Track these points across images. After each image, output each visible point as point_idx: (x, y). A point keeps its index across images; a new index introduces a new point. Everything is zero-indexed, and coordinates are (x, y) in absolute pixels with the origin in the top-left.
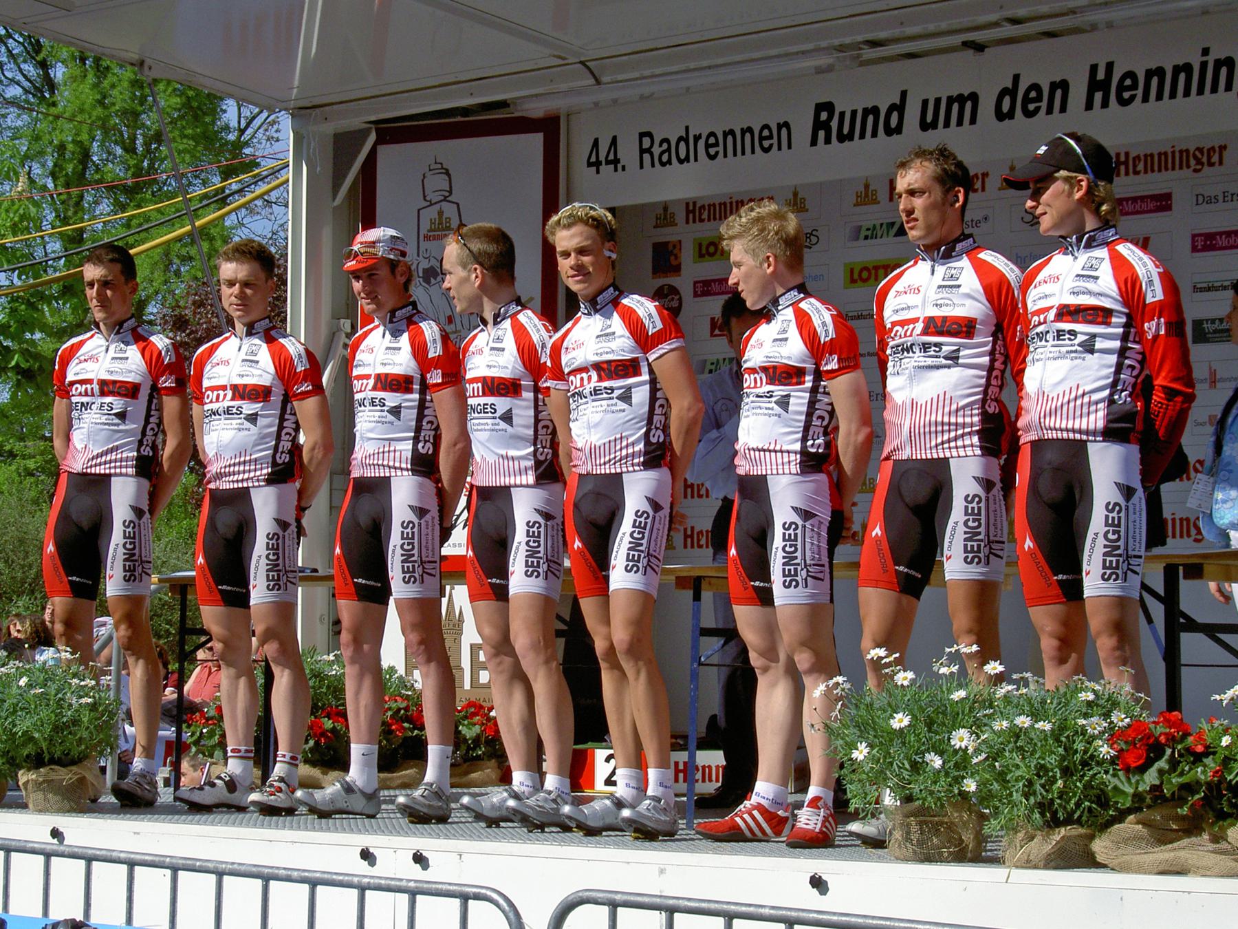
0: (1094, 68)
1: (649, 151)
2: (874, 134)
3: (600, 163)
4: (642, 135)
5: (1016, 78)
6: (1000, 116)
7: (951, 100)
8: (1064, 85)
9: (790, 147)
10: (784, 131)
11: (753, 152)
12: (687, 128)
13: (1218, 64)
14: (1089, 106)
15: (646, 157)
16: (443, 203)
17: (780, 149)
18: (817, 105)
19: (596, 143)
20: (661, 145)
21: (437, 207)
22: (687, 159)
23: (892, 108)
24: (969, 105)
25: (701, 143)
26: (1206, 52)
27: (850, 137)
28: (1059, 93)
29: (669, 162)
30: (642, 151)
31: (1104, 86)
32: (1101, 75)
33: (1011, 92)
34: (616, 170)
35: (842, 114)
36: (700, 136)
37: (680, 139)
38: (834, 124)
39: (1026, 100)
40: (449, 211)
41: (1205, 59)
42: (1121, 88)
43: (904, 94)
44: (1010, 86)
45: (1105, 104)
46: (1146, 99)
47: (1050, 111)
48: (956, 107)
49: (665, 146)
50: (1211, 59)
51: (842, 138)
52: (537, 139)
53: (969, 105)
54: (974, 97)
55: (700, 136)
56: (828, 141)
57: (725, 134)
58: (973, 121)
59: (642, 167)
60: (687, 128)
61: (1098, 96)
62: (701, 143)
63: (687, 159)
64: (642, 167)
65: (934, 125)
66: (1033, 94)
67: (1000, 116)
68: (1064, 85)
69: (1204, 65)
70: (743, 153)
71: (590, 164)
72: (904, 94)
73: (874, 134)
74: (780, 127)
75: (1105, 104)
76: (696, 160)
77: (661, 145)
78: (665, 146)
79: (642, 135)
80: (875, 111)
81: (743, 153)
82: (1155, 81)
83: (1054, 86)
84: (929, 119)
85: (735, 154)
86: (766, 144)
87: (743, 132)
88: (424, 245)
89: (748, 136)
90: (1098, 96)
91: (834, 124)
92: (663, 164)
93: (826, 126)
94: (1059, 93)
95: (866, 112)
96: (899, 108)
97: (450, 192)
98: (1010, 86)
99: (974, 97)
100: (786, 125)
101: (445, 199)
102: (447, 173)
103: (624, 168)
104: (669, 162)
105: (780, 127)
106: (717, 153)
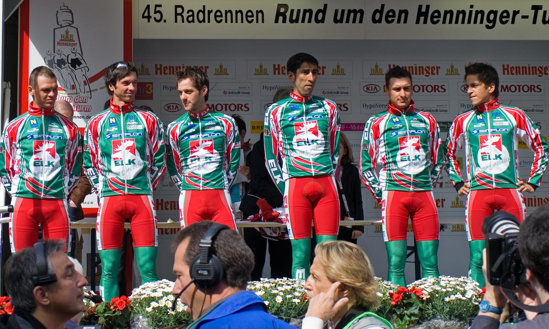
0: (420, 7)
1: (181, 14)
2: (310, 21)
3: (151, 17)
4: (176, 7)
5: (383, 6)
6: (374, 21)
7: (350, 12)
8: (406, 12)
9: (263, 22)
10: (260, 14)
11: (242, 22)
12: (204, 6)
13: (477, 12)
14: (418, 22)
15: (179, 17)
17: (257, 22)
18: (279, 5)
19: (148, 7)
20: (188, 12)
21: (65, 28)
22: (204, 21)
23: (319, 11)
24: (359, 15)
25: (212, 15)
26: (472, 7)
27: (297, 21)
29: (193, 21)
30: (177, 14)
31: (425, 14)
32: (423, 10)
33: (381, 12)
35: (292, 11)
36: (212, 11)
38: (288, 14)
39: (387, 16)
40: (72, 31)
41: (471, 9)
42: (433, 17)
43: (326, 6)
44: (380, 9)
45: (425, 22)
47: (399, 22)
48: (352, 15)
49: (191, 13)
50: (474, 10)
51: (291, 21)
53: (359, 15)
54: (361, 12)
55: (212, 11)
56: (284, 21)
57: (226, 12)
58: (361, 21)
59: (176, 21)
60: (204, 6)
61: (422, 19)
62: (212, 15)
63: (204, 21)
64: (176, 21)
65: (341, 21)
67: (374, 21)
68: (406, 12)
69: (471, 12)
70: (237, 22)
71: (144, 17)
72: (326, 6)
73: (310, 21)
74: (258, 12)
75: (425, 22)
76: (209, 22)
77: (188, 12)
78: (191, 13)
79: (176, 7)
80: (310, 11)
81: (237, 22)
82: (448, 16)
83: (401, 12)
84: (339, 18)
85: (232, 22)
86: (250, 19)
87: (237, 12)
89: (239, 14)
90: (422, 19)
91: (288, 14)
93: (284, 15)
95: (305, 11)
96: (324, 11)
97: (73, 22)
98: (380, 9)
99: (361, 12)
100: (261, 12)
101: (70, 25)
102: (71, 12)
103: (165, 21)
104: (193, 21)
105: (258, 12)
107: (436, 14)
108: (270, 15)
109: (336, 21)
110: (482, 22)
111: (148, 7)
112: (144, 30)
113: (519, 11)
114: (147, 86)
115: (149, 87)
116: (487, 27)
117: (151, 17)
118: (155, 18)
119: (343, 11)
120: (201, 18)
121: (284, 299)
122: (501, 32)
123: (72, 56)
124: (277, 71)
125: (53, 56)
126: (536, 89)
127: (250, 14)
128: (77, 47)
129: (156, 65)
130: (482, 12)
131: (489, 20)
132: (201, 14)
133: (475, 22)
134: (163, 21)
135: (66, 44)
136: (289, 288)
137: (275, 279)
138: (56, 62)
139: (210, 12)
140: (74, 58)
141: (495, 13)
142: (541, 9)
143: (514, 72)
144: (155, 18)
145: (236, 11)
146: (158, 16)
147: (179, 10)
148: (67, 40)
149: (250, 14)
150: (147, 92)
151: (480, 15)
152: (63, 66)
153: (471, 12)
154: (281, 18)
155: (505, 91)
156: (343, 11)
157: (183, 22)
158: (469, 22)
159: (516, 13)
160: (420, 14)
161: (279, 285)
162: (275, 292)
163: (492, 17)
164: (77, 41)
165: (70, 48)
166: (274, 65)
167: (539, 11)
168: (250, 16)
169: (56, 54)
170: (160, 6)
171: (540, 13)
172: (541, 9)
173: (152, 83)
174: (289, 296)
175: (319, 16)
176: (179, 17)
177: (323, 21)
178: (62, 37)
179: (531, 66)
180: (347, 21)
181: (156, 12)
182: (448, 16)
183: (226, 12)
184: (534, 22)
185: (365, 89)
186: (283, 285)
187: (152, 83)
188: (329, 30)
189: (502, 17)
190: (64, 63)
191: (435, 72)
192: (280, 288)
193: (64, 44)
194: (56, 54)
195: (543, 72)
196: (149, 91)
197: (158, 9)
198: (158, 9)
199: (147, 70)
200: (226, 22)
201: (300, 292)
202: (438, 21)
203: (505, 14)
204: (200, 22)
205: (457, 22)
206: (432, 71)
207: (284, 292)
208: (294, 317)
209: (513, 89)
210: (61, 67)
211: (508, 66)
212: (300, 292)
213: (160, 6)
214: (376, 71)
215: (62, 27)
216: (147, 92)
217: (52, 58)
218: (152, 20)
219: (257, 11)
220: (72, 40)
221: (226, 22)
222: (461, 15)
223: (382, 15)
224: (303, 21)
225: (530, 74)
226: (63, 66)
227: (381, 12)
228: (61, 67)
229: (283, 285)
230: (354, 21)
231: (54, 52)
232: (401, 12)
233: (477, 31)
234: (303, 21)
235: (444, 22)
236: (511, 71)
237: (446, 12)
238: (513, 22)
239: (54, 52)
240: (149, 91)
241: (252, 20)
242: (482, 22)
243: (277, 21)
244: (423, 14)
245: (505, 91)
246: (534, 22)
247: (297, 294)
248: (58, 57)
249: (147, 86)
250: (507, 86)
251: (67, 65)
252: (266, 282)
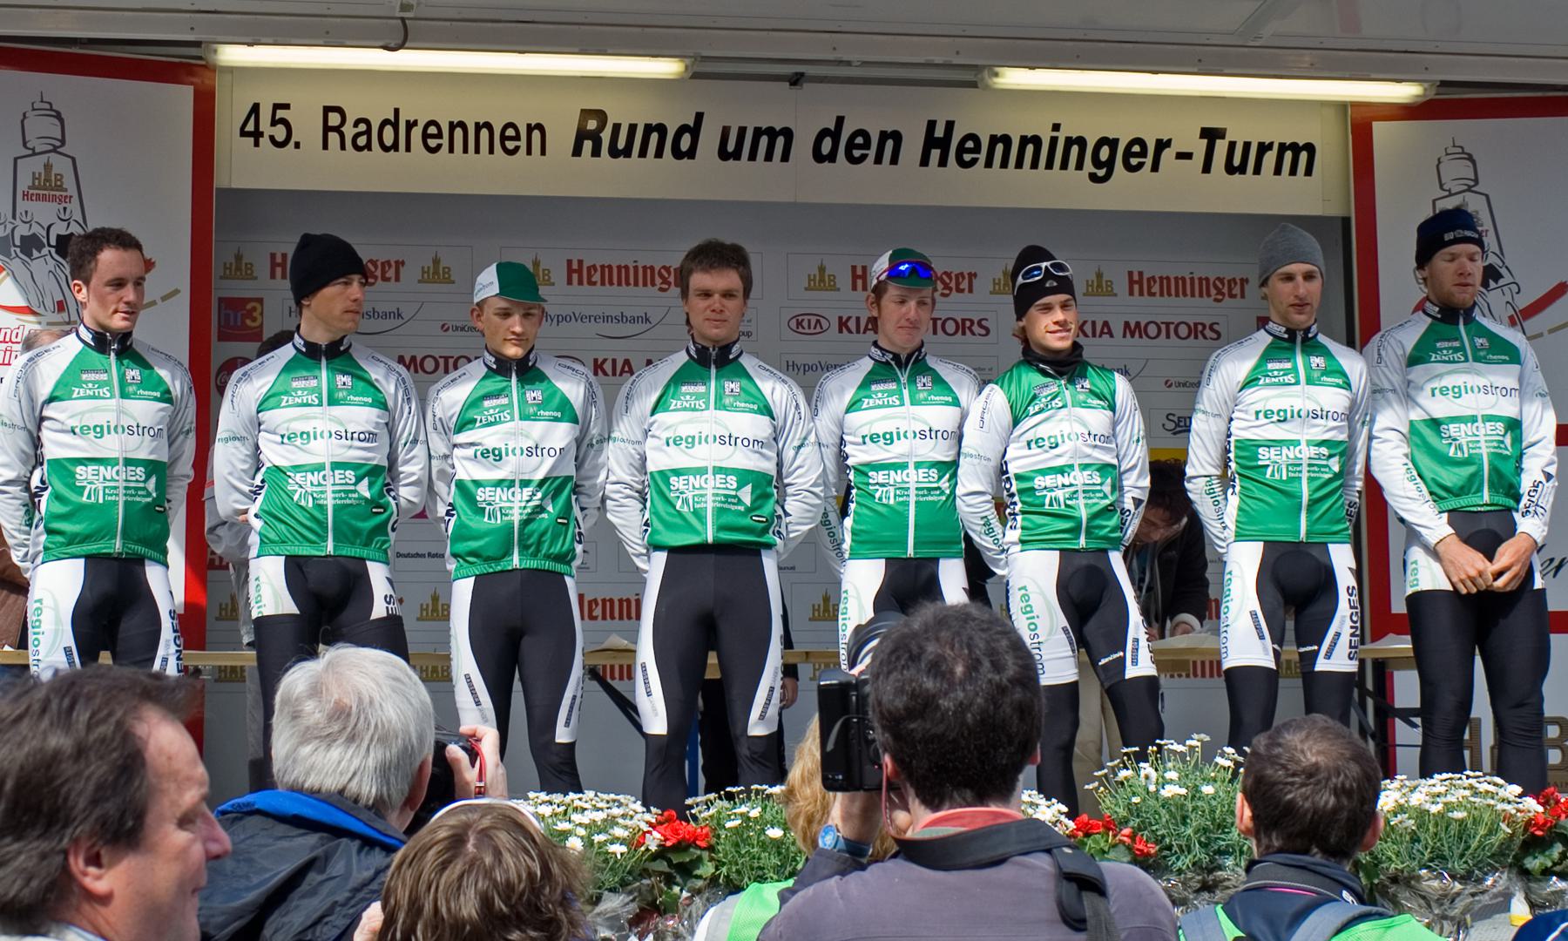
0: (932, 125)
1: (337, 129)
2: (659, 154)
3: (262, 134)
4: (327, 110)
5: (840, 121)
6: (818, 157)
7: (758, 132)
8: (897, 137)
9: (543, 152)
10: (536, 134)
11: (491, 151)
12: (397, 111)
13: (1069, 142)
14: (925, 162)
15: (334, 137)
16: (53, 157)
19: (255, 109)
20: (356, 125)
22: (395, 147)
23: (683, 129)
24: (780, 141)
25: (417, 133)
26: (1056, 127)
27: (627, 152)
28: (890, 144)
29: (368, 146)
30: (327, 129)
31: (944, 144)
32: (939, 132)
34: (257, 144)
35: (617, 127)
36: (415, 123)
37: (385, 122)
38: (606, 136)
39: (851, 145)
40: (61, 165)
42: (961, 149)
43: (699, 117)
45: (943, 162)
46: (878, 160)
47: (878, 160)
48: (764, 140)
49: (362, 127)
51: (614, 152)
52: (181, 97)
53: (780, 141)
54: (788, 133)
55: (415, 123)
56: (596, 152)
57: (452, 126)
59: (325, 147)
60: (397, 111)
61: (935, 154)
62: (417, 133)
63: (395, 147)
64: (325, 147)
65: (737, 155)
66: (859, 140)
67: (818, 157)
68: (897, 137)
69: (1054, 141)
70: (477, 151)
71: (243, 133)
72: (699, 117)
73: (659, 154)
74: (530, 129)
75: (943, 162)
76: (408, 149)
77: (356, 125)
78: (362, 127)
79: (327, 110)
80: (661, 129)
81: (477, 151)
82: (1000, 147)
83: (884, 136)
84: (731, 147)
85: (465, 150)
86: (510, 145)
87: (478, 127)
88: (22, 205)
89: (484, 133)
90: (935, 154)
91: (606, 136)
92: (358, 148)
94: (890, 144)
95: (649, 129)
96: (695, 131)
99: (788, 133)
100: (540, 127)
101: (55, 150)
102: (58, 116)
103: (297, 145)
104: (368, 146)
106: (439, 146)
107: (970, 144)
108: (562, 135)
109: (724, 154)
110: (1079, 166)
111: (255, 109)
112: (244, 166)
113: (1169, 141)
114: (249, 306)
115: (254, 309)
116: (1094, 178)
117: (262, 134)
118: (272, 138)
119: (742, 131)
120: (388, 141)
121: (589, 843)
122: (1128, 191)
123: (60, 229)
124: (575, 276)
125: (9, 227)
126: (1208, 333)
127: (510, 132)
128: (74, 206)
129: (273, 256)
130: (1081, 142)
131: (1097, 162)
132: (388, 132)
133: (1064, 166)
134: (292, 144)
135: (45, 198)
136: (599, 816)
137: (566, 794)
138: (18, 242)
139: (410, 125)
140: (64, 232)
141: (1113, 144)
142: (1223, 137)
143: (1156, 289)
144: (272, 138)
145: (477, 124)
146: (280, 133)
147: (334, 119)
148: (47, 187)
149: (510, 132)
150: (248, 322)
151: (1075, 149)
152: (35, 253)
153: (1054, 141)
154: (588, 145)
155: (1133, 336)
156: (742, 131)
157: (343, 147)
158: (1049, 166)
159: (1162, 145)
160: (930, 142)
161: (576, 809)
162: (563, 826)
163: (1104, 153)
164: (72, 191)
165: (54, 207)
166: (570, 262)
167: (1218, 142)
168: (511, 138)
169: (18, 222)
170: (286, 106)
171: (1221, 147)
172: (1223, 137)
173: (260, 301)
174: (597, 838)
175: (681, 142)
176: (334, 137)
177: (691, 153)
178: (34, 178)
179: (1196, 276)
180: (752, 157)
181: (274, 123)
182: (1000, 147)
183: (452, 126)
184: (1207, 169)
185: (793, 324)
186: (584, 810)
187: (260, 301)
188: (703, 178)
189: (1128, 154)
190: (40, 247)
191: (964, 285)
192: (576, 817)
193: (38, 198)
194: (18, 222)
195: (1225, 290)
196: (254, 320)
197: (280, 114)
198: (280, 114)
199: (250, 266)
200: (451, 150)
201: (626, 827)
202: (974, 161)
203: (1136, 148)
204: (386, 149)
205: (1019, 165)
206: (958, 284)
207: (586, 827)
208: (610, 890)
209: (1152, 330)
210: (30, 255)
211: (1141, 274)
212: (626, 827)
213: (286, 106)
214: (822, 281)
215: (34, 154)
216: (248, 322)
217: (9, 231)
218: (264, 141)
219: (529, 126)
220: (60, 188)
221: (451, 150)
222: (1030, 148)
223: (836, 143)
224: (643, 153)
225: (1193, 295)
226: (35, 253)
227: (835, 135)
228: (30, 255)
229: (584, 810)
230: (769, 157)
231: (14, 217)
232: (884, 136)
233: (1068, 189)
234: (643, 153)
235: (989, 164)
236: (1149, 288)
237: (994, 140)
238: (1155, 168)
239: (14, 217)
240: (254, 320)
241: (517, 148)
242: (1079, 166)
243: (577, 151)
244: (936, 143)
245: (1133, 336)
246: (1207, 169)
247: (619, 832)
248: (22, 230)
249: (249, 306)
250: (1138, 324)
251: (45, 251)
252: (544, 802)
